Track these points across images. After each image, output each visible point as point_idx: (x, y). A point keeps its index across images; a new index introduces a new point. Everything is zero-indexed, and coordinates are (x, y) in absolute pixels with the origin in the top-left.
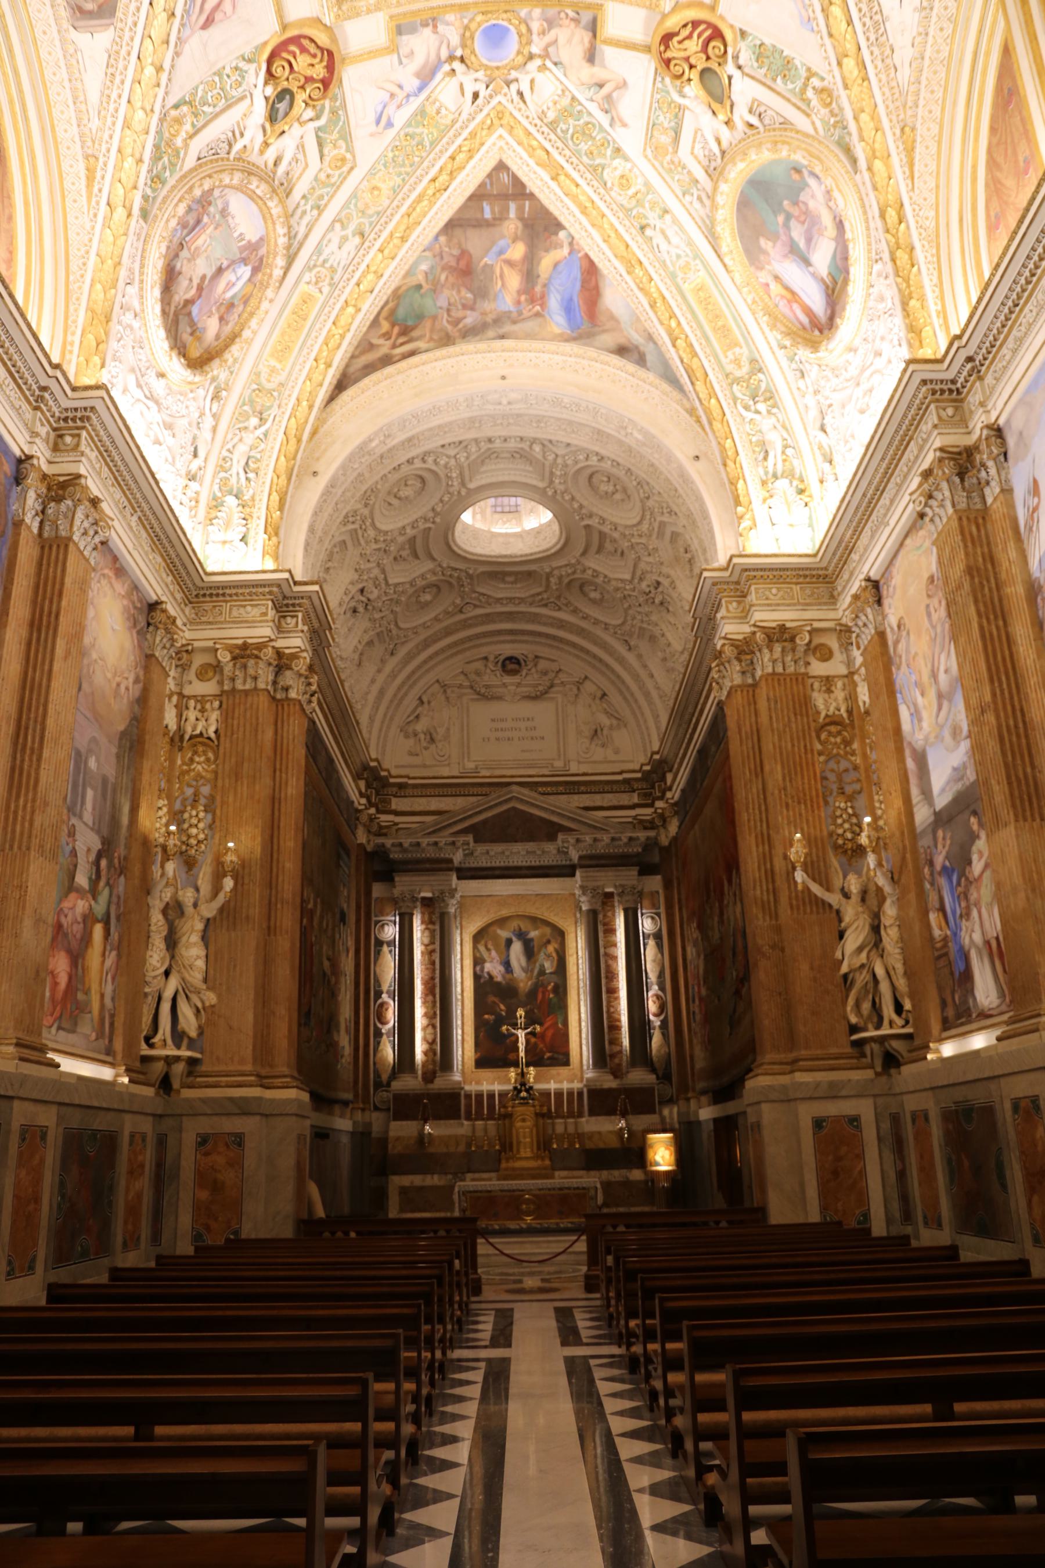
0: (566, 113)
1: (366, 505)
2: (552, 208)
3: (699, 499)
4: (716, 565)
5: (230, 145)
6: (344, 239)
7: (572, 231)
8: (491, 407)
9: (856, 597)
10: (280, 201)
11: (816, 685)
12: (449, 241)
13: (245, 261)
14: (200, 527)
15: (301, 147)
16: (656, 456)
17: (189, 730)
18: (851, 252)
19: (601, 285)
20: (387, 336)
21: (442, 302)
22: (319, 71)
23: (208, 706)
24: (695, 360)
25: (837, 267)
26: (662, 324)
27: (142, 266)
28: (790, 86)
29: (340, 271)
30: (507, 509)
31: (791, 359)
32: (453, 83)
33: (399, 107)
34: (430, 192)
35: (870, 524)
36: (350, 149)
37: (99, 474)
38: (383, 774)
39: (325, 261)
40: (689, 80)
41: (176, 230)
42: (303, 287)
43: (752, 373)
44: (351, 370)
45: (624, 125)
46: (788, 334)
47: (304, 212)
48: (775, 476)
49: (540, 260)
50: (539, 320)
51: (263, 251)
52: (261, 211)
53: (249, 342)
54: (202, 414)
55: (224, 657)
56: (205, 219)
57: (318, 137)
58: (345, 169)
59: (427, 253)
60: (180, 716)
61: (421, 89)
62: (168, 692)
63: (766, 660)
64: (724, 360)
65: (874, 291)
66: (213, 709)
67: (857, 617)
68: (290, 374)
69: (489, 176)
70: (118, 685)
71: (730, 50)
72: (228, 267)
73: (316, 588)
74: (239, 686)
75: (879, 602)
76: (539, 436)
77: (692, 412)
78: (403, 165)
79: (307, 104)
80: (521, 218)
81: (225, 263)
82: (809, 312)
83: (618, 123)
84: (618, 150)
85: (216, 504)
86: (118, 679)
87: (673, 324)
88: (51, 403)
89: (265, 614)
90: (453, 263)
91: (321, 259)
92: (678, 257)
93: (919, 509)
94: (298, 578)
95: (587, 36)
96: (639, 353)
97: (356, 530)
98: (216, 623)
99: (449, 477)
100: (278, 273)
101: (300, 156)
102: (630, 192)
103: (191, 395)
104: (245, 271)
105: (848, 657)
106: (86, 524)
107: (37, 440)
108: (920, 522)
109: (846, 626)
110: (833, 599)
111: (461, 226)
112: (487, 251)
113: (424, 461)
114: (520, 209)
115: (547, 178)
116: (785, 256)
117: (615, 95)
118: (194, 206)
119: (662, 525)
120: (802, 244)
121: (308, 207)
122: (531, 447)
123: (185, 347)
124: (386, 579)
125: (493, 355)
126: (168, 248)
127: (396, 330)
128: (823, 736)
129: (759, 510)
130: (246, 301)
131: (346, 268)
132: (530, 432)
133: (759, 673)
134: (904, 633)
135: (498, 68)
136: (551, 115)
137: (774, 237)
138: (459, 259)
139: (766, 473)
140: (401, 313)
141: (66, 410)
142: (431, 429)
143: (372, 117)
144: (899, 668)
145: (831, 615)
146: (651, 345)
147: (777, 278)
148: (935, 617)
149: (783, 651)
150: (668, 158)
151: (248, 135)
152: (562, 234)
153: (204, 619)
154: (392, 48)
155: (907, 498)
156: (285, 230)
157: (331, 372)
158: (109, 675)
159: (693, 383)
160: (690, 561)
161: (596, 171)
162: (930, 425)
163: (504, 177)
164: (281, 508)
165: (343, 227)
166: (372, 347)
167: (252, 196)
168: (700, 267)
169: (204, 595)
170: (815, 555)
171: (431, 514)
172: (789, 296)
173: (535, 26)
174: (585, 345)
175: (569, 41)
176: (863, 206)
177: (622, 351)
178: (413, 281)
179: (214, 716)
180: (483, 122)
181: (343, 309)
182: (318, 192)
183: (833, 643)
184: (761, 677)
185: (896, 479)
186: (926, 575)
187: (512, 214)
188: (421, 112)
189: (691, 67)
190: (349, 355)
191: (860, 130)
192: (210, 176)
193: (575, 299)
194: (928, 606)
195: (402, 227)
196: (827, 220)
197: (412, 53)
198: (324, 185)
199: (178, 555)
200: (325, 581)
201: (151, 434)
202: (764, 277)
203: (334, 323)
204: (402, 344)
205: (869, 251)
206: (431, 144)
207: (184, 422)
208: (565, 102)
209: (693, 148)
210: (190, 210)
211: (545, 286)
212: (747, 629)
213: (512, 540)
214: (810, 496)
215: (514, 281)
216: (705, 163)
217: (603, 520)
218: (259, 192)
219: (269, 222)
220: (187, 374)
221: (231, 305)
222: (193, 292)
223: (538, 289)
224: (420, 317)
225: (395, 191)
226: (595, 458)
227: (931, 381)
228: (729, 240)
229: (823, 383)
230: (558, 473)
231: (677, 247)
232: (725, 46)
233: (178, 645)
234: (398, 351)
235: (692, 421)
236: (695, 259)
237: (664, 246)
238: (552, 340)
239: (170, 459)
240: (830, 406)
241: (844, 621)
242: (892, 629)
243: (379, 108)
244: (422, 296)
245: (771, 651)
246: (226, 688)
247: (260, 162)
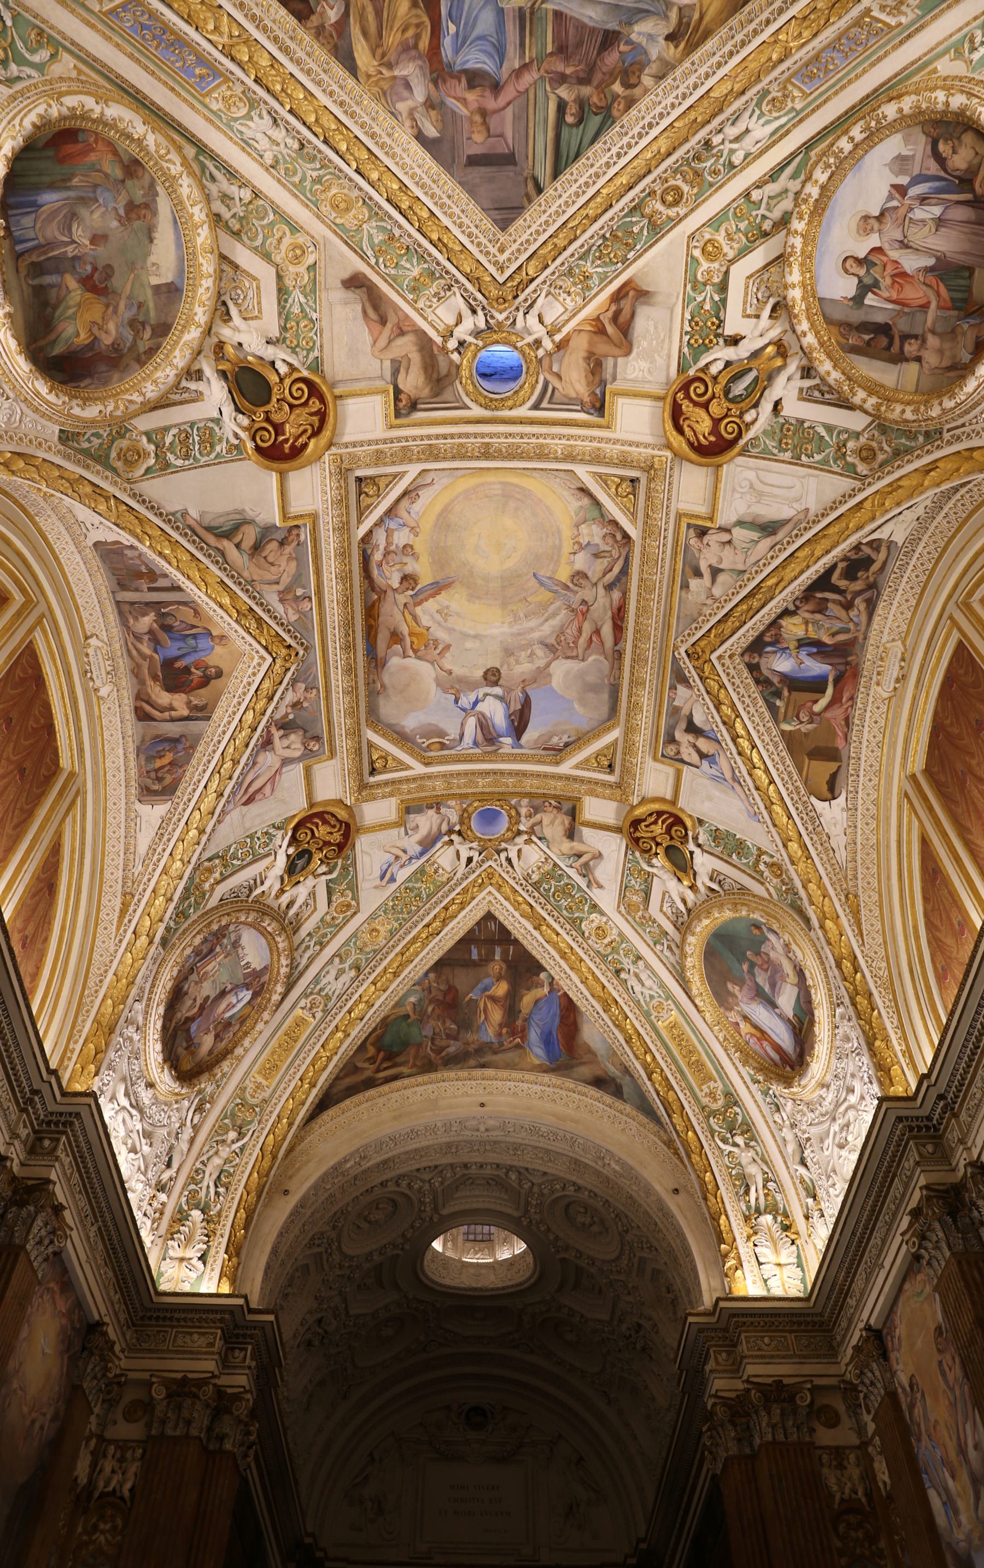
0: (547, 876)
1: (334, 1228)
2: (534, 953)
3: (681, 1235)
4: (701, 1308)
5: (251, 891)
6: (341, 972)
7: (552, 972)
8: (469, 1133)
9: (857, 1349)
10: (288, 936)
11: (825, 1458)
12: (438, 977)
13: (247, 986)
14: (160, 1241)
15: (312, 895)
16: (634, 1187)
17: (101, 1484)
18: (813, 996)
19: (579, 1021)
20: (372, 1060)
21: (428, 1031)
22: (337, 837)
23: (129, 1454)
24: (671, 1093)
25: (802, 1009)
26: (637, 1058)
27: (153, 986)
28: (745, 861)
29: (334, 999)
30: (479, 1237)
31: (765, 1093)
32: (451, 851)
33: (402, 867)
34: (424, 936)
35: (862, 1266)
36: (355, 898)
37: (69, 1180)
38: (319, 1554)
39: (321, 990)
40: (657, 854)
41: (189, 957)
42: (298, 1012)
43: (727, 1106)
44: (335, 1090)
45: (600, 887)
46: (760, 1069)
47: (308, 947)
48: (759, 1212)
50: (519, 1051)
51: (265, 978)
52: (269, 944)
53: (240, 1059)
54: (183, 1125)
55: (159, 1393)
56: (218, 949)
57: (328, 886)
58: (349, 913)
59: (417, 987)
60: (94, 1465)
61: (422, 854)
62: (87, 1433)
63: (764, 1425)
64: (699, 1094)
65: (840, 1031)
66: (134, 1460)
67: (862, 1373)
68: (274, 1091)
69: (478, 924)
70: (33, 1422)
71: (690, 834)
72: (231, 990)
73: (271, 1318)
74: (169, 1432)
75: (885, 1355)
76: (515, 1163)
77: (669, 1143)
78: (402, 912)
79: (322, 862)
80: (505, 959)
81: (229, 987)
82: (778, 1048)
84: (595, 907)
85: (181, 1217)
86: (34, 1415)
87: (649, 1059)
88: (39, 1106)
89: (212, 1345)
90: (440, 998)
91: (318, 987)
92: (652, 997)
93: (913, 1250)
94: (254, 1305)
97: (320, 1254)
98: (157, 1351)
99: (423, 1203)
100: (276, 998)
101: (311, 902)
102: (606, 941)
103: (175, 1106)
104: (246, 995)
105: (858, 1421)
106: (43, 1233)
107: (16, 1142)
108: (916, 1265)
109: (851, 1383)
110: (831, 1351)
111: (450, 965)
112: (472, 989)
113: (398, 1185)
114: (505, 953)
115: (530, 927)
116: (752, 999)
118: (210, 938)
119: (642, 1260)
120: (767, 989)
121: (312, 943)
122: (507, 1174)
123: (178, 1060)
124: (346, 1309)
125: (473, 1083)
126: (180, 971)
127: (381, 1055)
128: (842, 1528)
129: (744, 1249)
130: (243, 1021)
131: (340, 997)
132: (507, 1160)
133: (757, 1441)
134: (919, 1395)
135: (490, 840)
136: (535, 877)
137: (740, 982)
138: (446, 993)
139: (749, 1208)
140: (388, 1039)
141: (52, 1114)
142: (407, 1153)
143: (378, 873)
144: (919, 1440)
145: (833, 1370)
146: (627, 1077)
147: (746, 1018)
148: (951, 1377)
149: (782, 1414)
150: (640, 913)
151: (267, 884)
152: (543, 975)
153: (145, 1346)
154: (400, 823)
155: (898, 1239)
156: (289, 962)
157: (315, 1091)
158: (25, 1410)
159: (669, 1116)
160: (673, 1302)
161: (575, 923)
162: (912, 1161)
163: (492, 926)
164: (246, 1228)
165: (342, 962)
166: (356, 1070)
167: (263, 932)
168: (673, 1006)
169: (150, 1318)
170: (807, 1299)
171: (400, 1241)
172: (758, 1034)
173: (523, 811)
174: (563, 1076)
175: (552, 823)
176: (820, 958)
177: (600, 1082)
178: (401, 1011)
179: (134, 1468)
180: (475, 881)
181: (333, 1033)
182: (323, 931)
183: (841, 1408)
184: (761, 1446)
185: (884, 1217)
186: (933, 1327)
187: (497, 957)
188: (421, 871)
189: (658, 844)
190: (333, 1077)
191: (809, 896)
192: (228, 914)
194: (940, 1363)
195: (395, 965)
196: (788, 968)
197: (417, 827)
198: (329, 925)
199: (131, 1271)
200: (282, 1308)
201: (130, 1142)
202: (733, 1017)
203: (323, 1046)
204: (385, 1069)
205: (830, 996)
206: (428, 896)
207: (164, 1132)
208: (548, 867)
209: (662, 906)
210: (205, 940)
211: (525, 1020)
212: (740, 1385)
213: (483, 1271)
214: (797, 1233)
215: (497, 1015)
216: (673, 918)
217: (580, 1254)
218: (269, 929)
219: (275, 954)
220: (176, 1087)
221: (228, 1024)
222: (196, 1010)
223: (519, 1023)
224: (405, 1044)
225: (392, 933)
226: (572, 1188)
227: (907, 1118)
228: (698, 984)
229: (798, 1117)
230: (534, 1202)
231: (651, 989)
232: (686, 829)
233: (110, 1375)
234: (381, 1075)
235: (669, 1153)
236: (667, 1000)
237: (638, 988)
238: (531, 1070)
239: (143, 1168)
240: (808, 1139)
241: (848, 1377)
242: (904, 1389)
243: (385, 867)
244: (409, 1025)
245: (769, 1413)
246: (153, 1432)
247: (275, 905)
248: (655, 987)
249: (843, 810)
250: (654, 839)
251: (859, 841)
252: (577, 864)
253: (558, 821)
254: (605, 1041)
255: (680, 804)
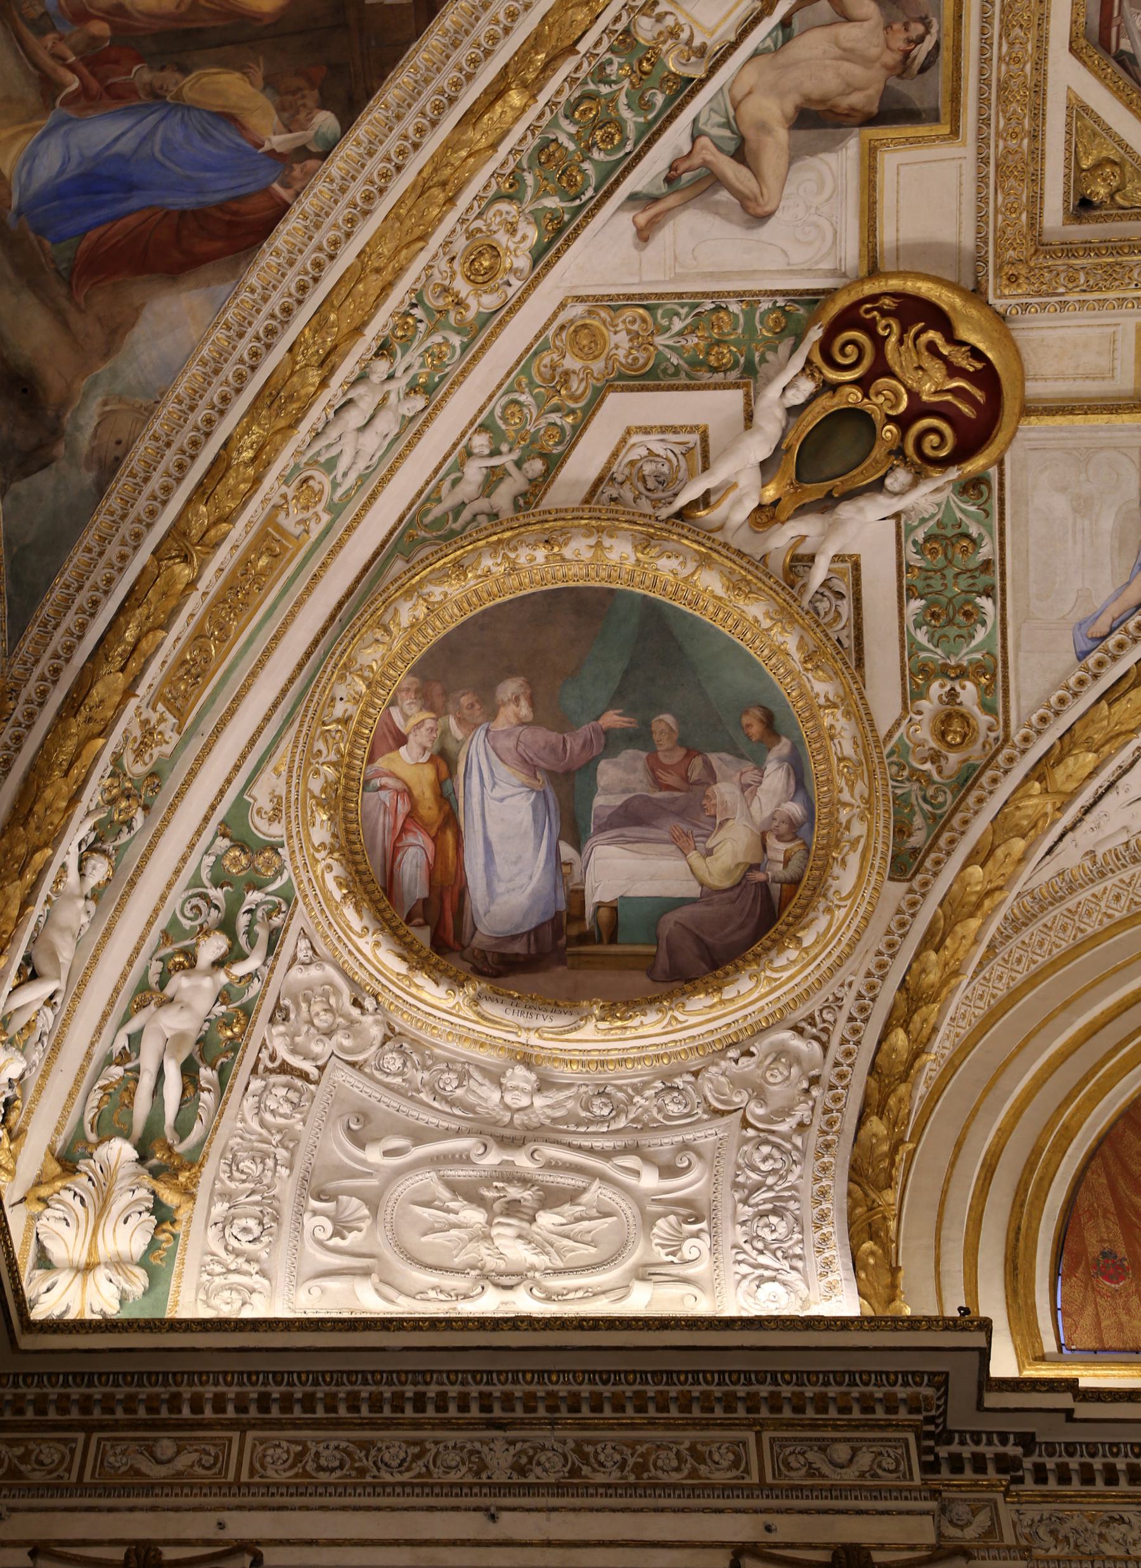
2: (401, 80)
28: (921, 636)
45: (644, 235)
49: (241, 69)
50: (32, 97)
83: (642, 219)
92: (330, 465)
95: (864, 99)
96: (41, 446)
117: (724, 195)
136: (646, 29)
152: (325, 121)
168: (316, 530)
193: (135, 202)
209: (647, 431)
211: (156, 95)
216: (619, 469)
223: (141, 74)
236: (329, 509)
248: (361, 465)
249: (1125, 828)
250: (881, 369)
251: (1084, 895)
252: (708, 152)
253: (857, 72)
254: (173, 372)
255: (1034, 429)
